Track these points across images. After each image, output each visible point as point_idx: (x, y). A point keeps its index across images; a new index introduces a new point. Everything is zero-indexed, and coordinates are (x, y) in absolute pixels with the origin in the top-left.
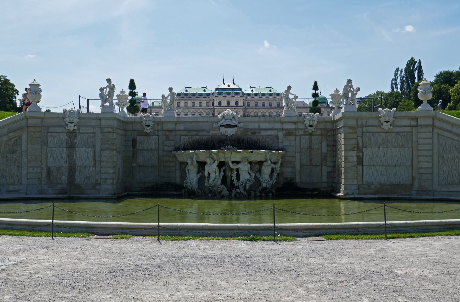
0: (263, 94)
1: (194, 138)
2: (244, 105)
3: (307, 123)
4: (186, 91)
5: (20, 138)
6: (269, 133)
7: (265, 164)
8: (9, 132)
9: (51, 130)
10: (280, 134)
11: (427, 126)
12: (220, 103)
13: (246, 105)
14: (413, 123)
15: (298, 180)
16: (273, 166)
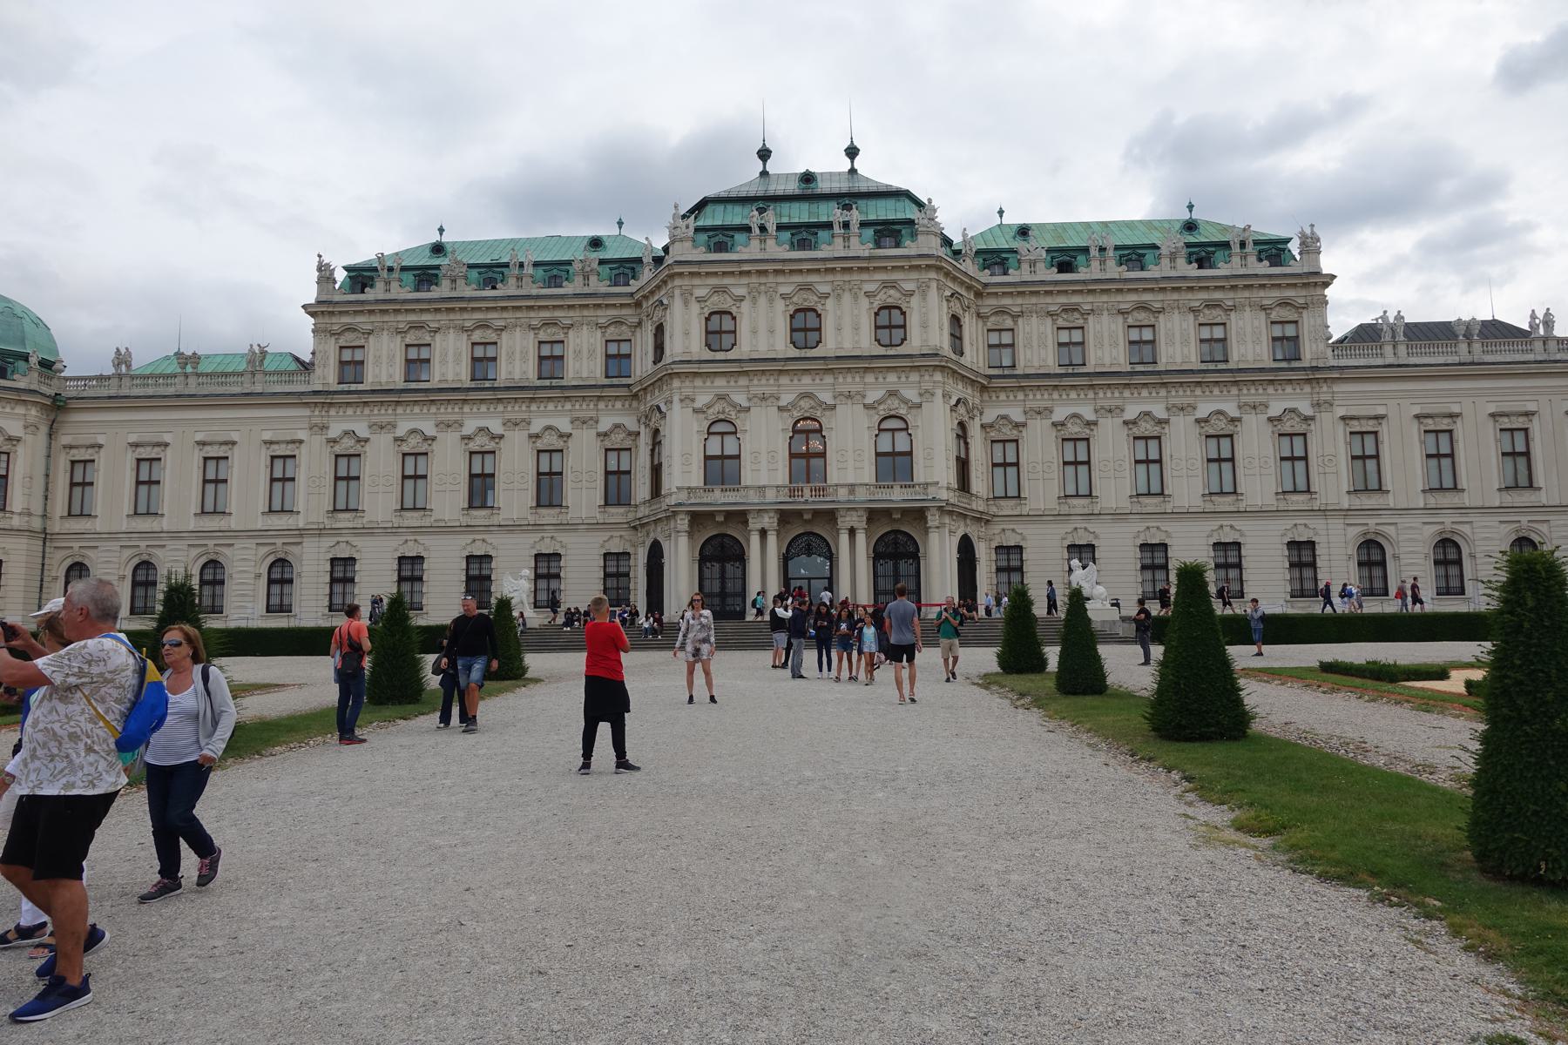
0: (1134, 255)
4: (438, 249)
12: (719, 329)
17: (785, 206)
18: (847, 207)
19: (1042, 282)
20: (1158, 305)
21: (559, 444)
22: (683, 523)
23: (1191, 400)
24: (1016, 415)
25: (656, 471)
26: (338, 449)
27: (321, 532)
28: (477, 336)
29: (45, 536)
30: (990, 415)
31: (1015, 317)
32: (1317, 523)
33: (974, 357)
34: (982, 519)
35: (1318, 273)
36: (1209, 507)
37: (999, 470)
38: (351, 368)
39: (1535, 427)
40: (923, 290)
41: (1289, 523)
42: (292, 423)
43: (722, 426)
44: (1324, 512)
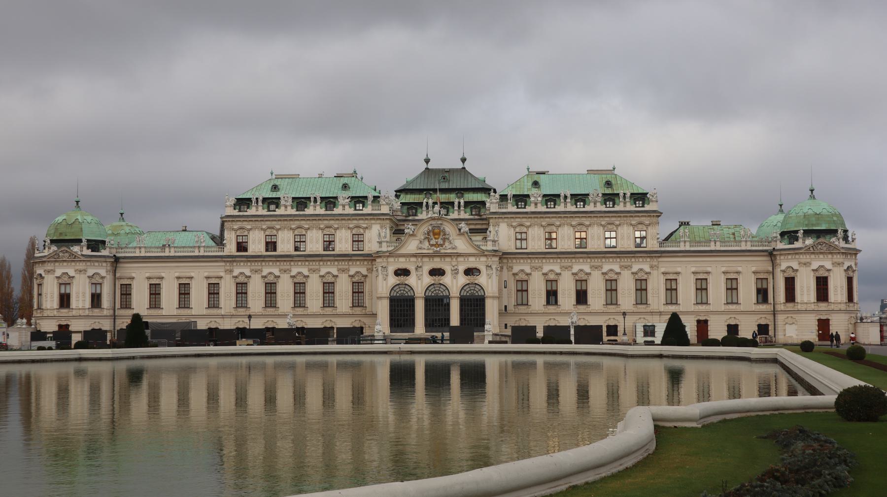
4: (275, 188)
19: (540, 213)
20: (588, 223)
21: (333, 280)
23: (600, 264)
24: (528, 270)
26: (238, 280)
27: (232, 316)
28: (296, 232)
29: (114, 317)
31: (528, 227)
35: (655, 211)
36: (605, 310)
37: (520, 293)
38: (242, 247)
42: (217, 269)
44: (652, 313)
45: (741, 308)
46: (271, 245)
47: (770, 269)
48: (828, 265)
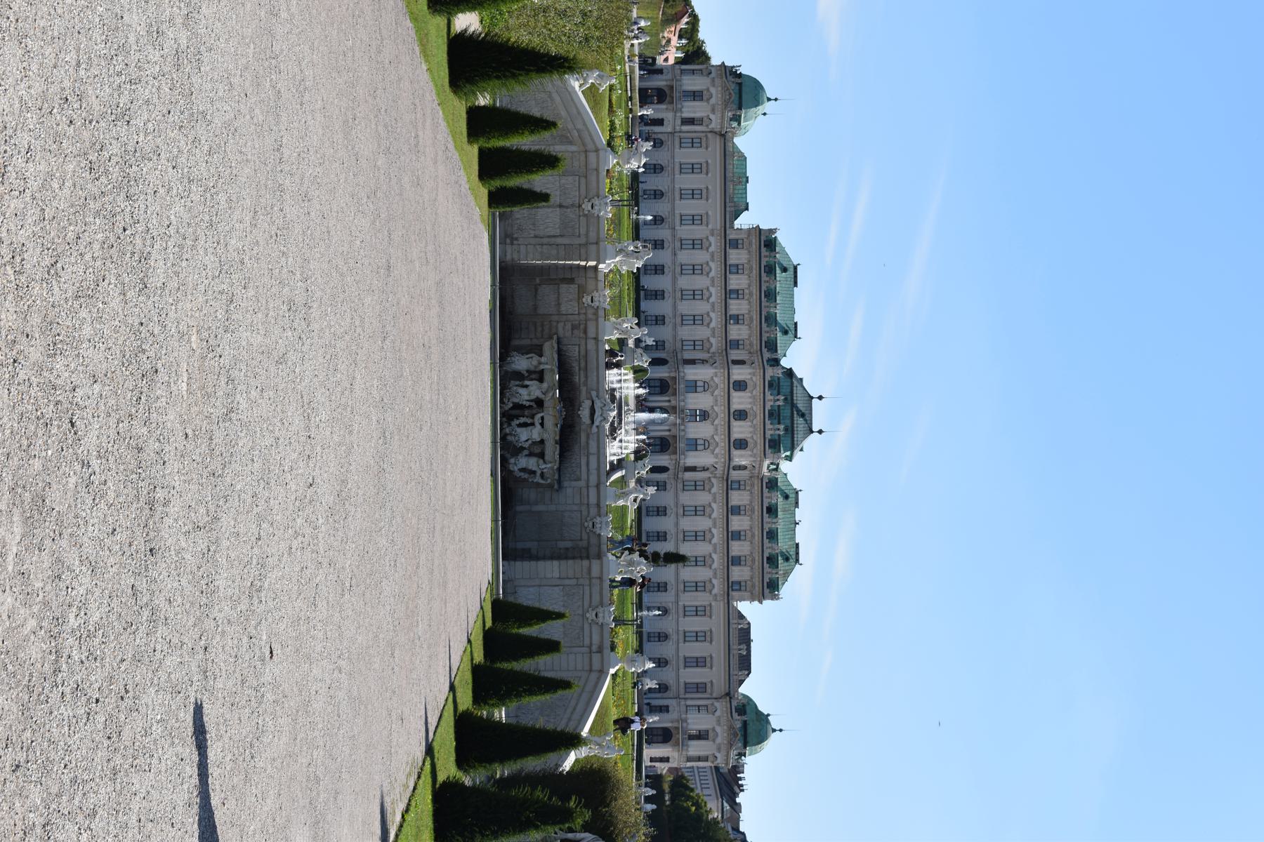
0: (772, 535)
1: (575, 364)
2: (735, 468)
3: (598, 520)
4: (785, 270)
5: (571, 143)
6: (584, 468)
7: (541, 461)
8: (578, 131)
9: (583, 180)
10: (582, 483)
11: (591, 665)
12: (741, 386)
13: (735, 475)
14: (594, 648)
15: (519, 508)
16: (539, 472)
17: (789, 407)
18: (786, 429)
22: (673, 375)
24: (714, 490)
25: (692, 362)
29: (672, 133)
30: (714, 480)
32: (673, 592)
33: (735, 475)
34: (676, 477)
38: (735, 244)
39: (706, 670)
40: (754, 456)
41: (673, 582)
42: (716, 222)
43: (706, 387)
44: (677, 595)
45: (682, 670)
46: (737, 269)
47: (715, 695)
48: (719, 740)
